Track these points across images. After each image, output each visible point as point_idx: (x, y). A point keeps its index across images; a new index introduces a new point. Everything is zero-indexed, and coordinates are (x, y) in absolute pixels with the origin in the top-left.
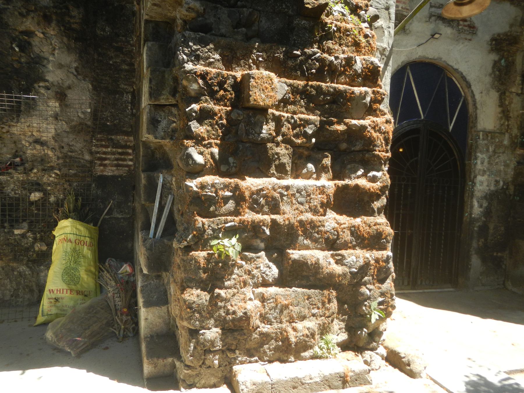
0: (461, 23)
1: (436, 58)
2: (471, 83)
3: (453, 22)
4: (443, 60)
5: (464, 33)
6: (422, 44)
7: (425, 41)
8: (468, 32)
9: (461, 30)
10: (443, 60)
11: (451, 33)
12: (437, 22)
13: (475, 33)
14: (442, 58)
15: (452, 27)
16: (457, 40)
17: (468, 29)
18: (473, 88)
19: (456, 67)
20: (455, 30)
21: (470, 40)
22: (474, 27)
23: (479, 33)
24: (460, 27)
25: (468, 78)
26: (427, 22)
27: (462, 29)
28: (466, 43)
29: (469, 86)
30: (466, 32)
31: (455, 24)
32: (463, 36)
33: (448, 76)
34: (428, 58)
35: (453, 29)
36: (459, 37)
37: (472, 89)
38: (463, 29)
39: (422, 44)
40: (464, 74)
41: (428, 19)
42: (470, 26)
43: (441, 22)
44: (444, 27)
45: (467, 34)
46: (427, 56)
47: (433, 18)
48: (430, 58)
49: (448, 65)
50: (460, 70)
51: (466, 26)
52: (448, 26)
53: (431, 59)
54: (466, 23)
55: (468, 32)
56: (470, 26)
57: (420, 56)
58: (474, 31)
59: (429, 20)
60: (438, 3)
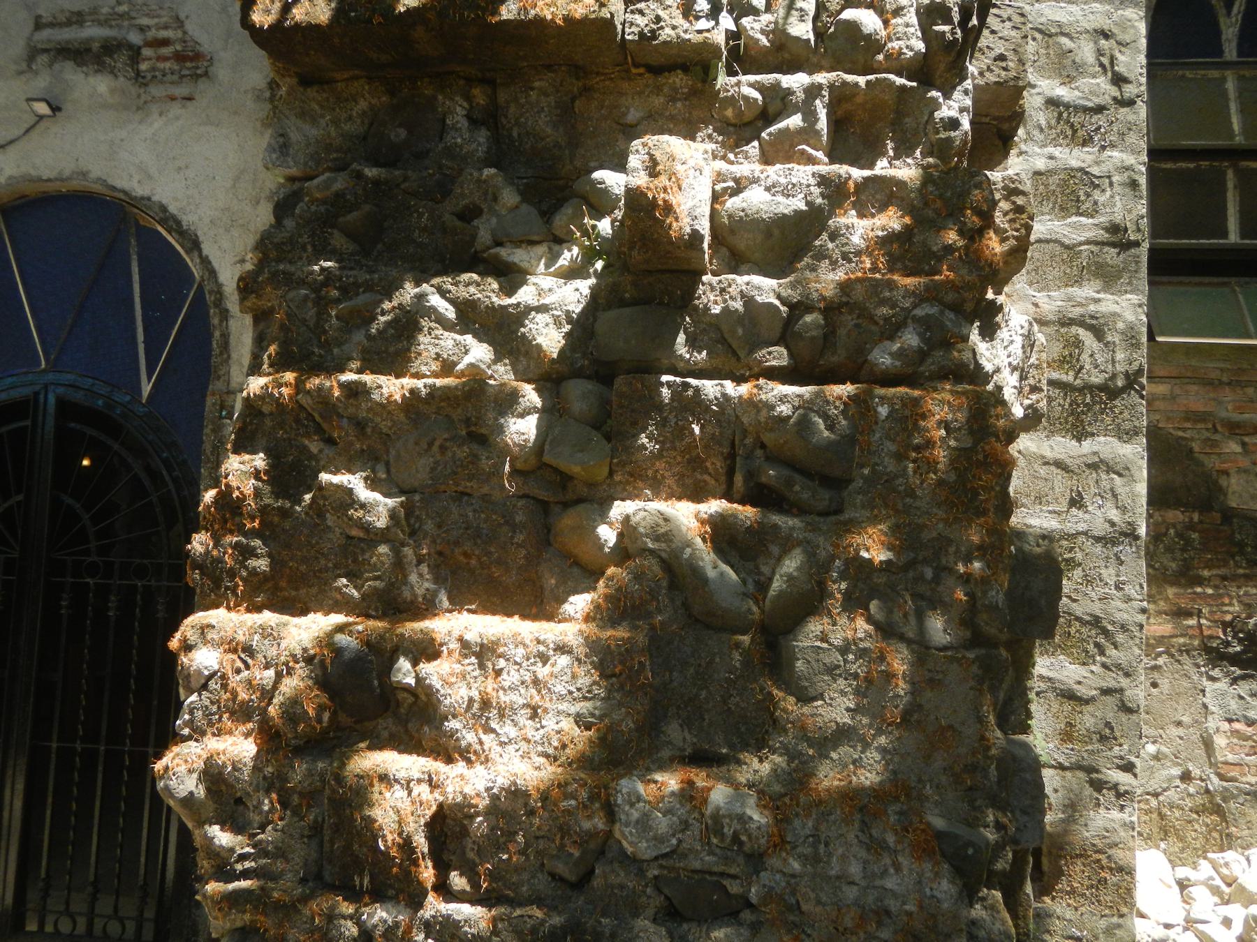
0: (147, 52)
1: (67, 173)
2: (199, 233)
3: (111, 56)
4: (93, 175)
5: (162, 82)
6: (11, 142)
7: (22, 131)
8: (175, 77)
9: (149, 76)
10: (93, 175)
11: (112, 91)
12: (57, 66)
13: (206, 74)
14: (88, 172)
15: (113, 72)
16: (139, 108)
17: (176, 67)
18: (207, 249)
19: (140, 191)
20: (122, 79)
21: (190, 99)
22: (197, 56)
23: (222, 72)
24: (143, 66)
25: (188, 220)
26: (21, 73)
27: (153, 69)
28: (175, 109)
29: (194, 245)
30: (169, 77)
31: (121, 59)
32: (156, 90)
33: (142, 223)
34: (40, 180)
35: (116, 76)
36: (144, 97)
37: (205, 252)
38: (159, 70)
39: (11, 142)
40: (173, 209)
41: (24, 65)
42: (180, 57)
43: (69, 65)
44: (82, 76)
45: (172, 83)
46: (33, 173)
47: (43, 59)
48: (44, 178)
49: (114, 188)
50: (155, 198)
51: (166, 59)
52: (96, 71)
53: (49, 180)
54: (166, 51)
55: (175, 77)
56: (180, 57)
57: (10, 178)
58: (197, 68)
59: (29, 66)
60: (62, 11)
